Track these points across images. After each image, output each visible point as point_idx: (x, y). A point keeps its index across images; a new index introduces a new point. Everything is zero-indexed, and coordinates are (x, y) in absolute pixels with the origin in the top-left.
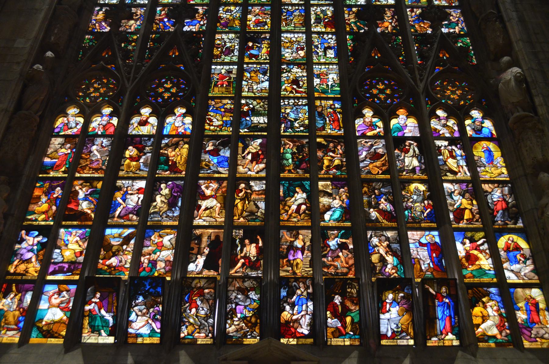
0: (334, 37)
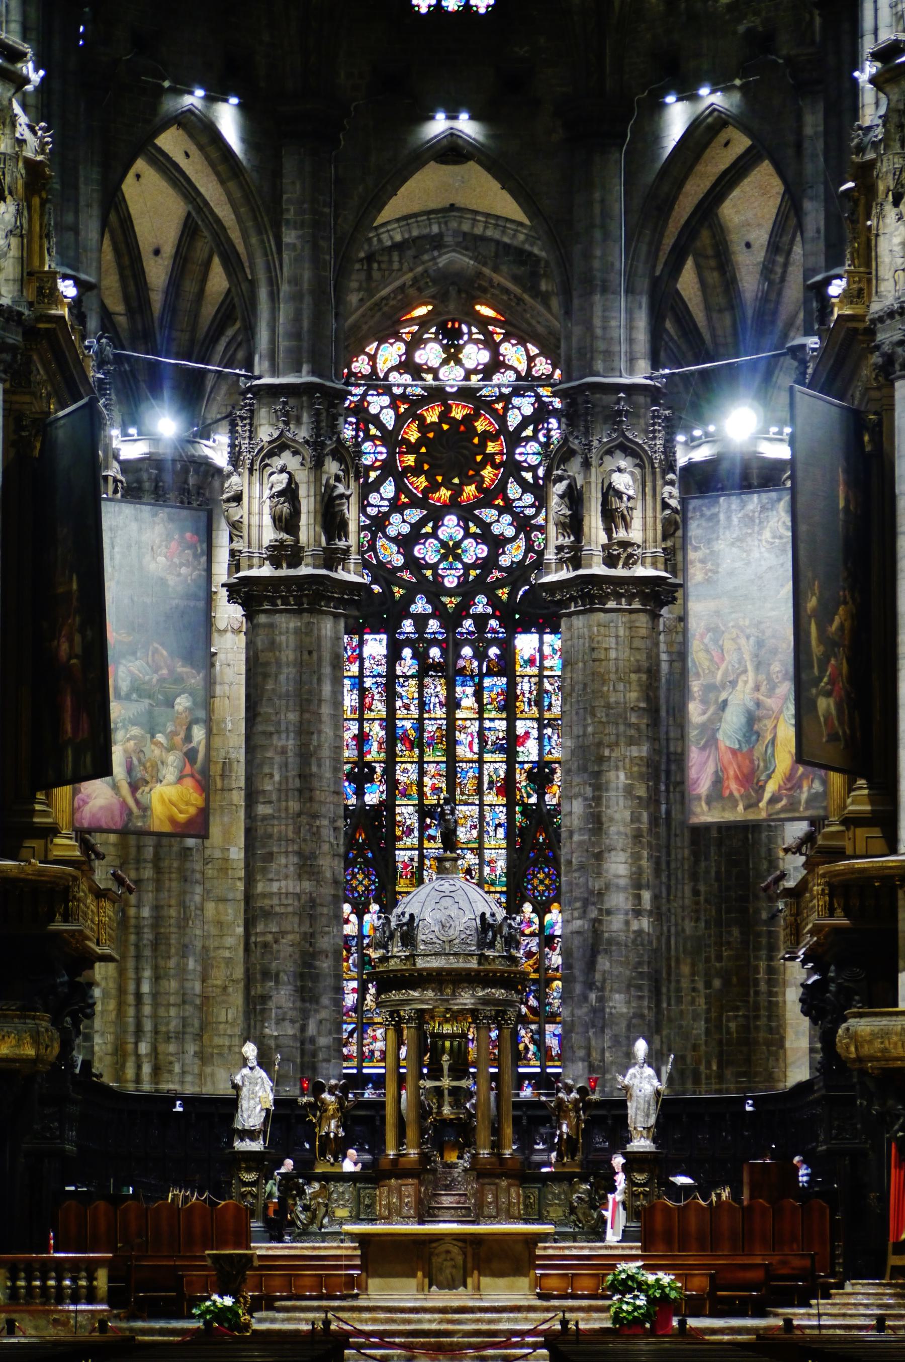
0: (504, 810)
